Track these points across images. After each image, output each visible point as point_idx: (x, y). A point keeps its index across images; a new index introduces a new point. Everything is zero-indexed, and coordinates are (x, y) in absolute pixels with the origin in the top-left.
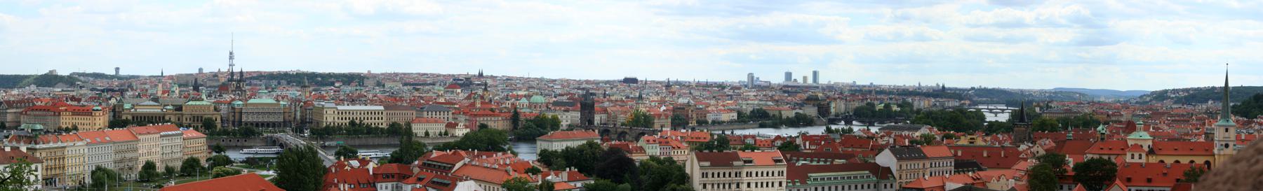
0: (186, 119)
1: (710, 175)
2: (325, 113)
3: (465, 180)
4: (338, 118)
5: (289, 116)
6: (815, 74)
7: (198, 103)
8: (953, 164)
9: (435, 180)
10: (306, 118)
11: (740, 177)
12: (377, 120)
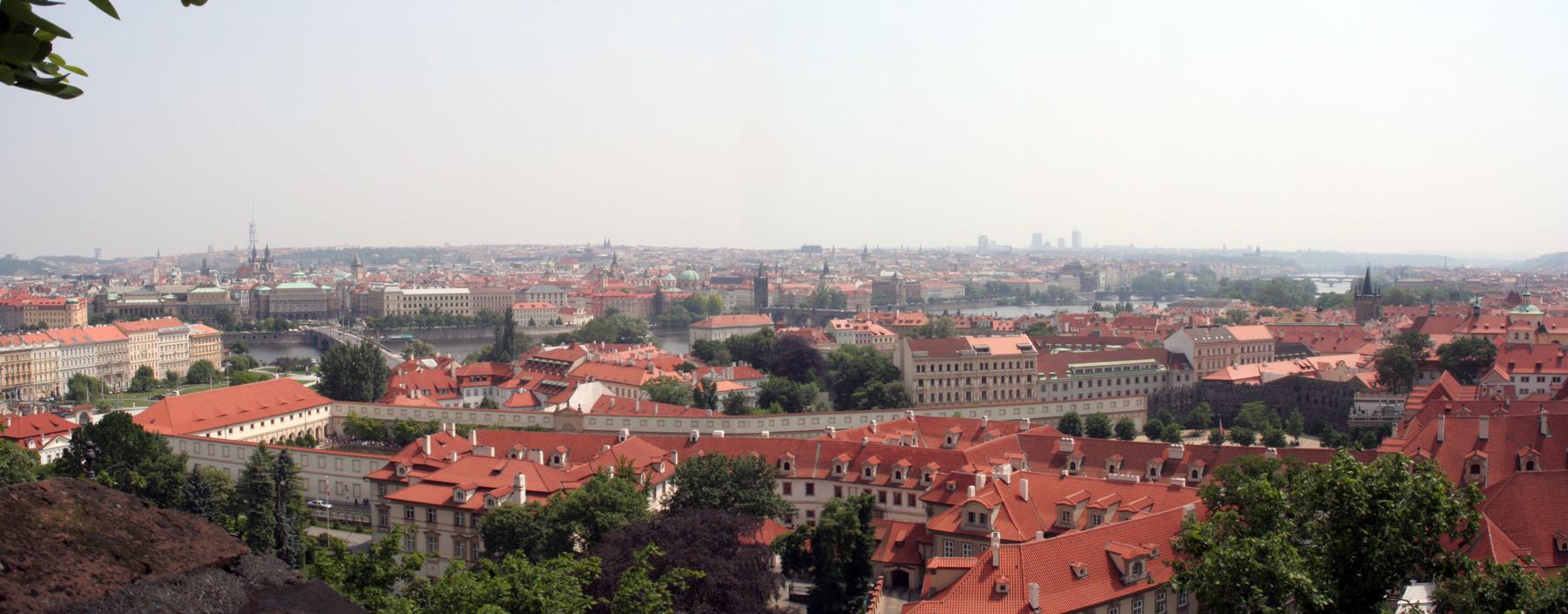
0: (193, 312)
1: (928, 369)
2: (385, 298)
3: (588, 382)
4: (405, 306)
5: (336, 304)
6: (1076, 235)
7: (208, 290)
9: (544, 382)
10: (359, 307)
12: (460, 307)
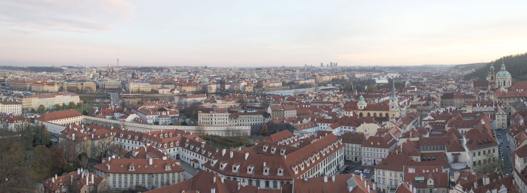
8: (296, 112)
11: (212, 116)
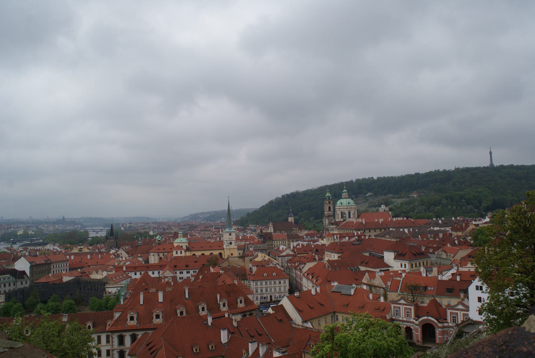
8: (68, 265)
